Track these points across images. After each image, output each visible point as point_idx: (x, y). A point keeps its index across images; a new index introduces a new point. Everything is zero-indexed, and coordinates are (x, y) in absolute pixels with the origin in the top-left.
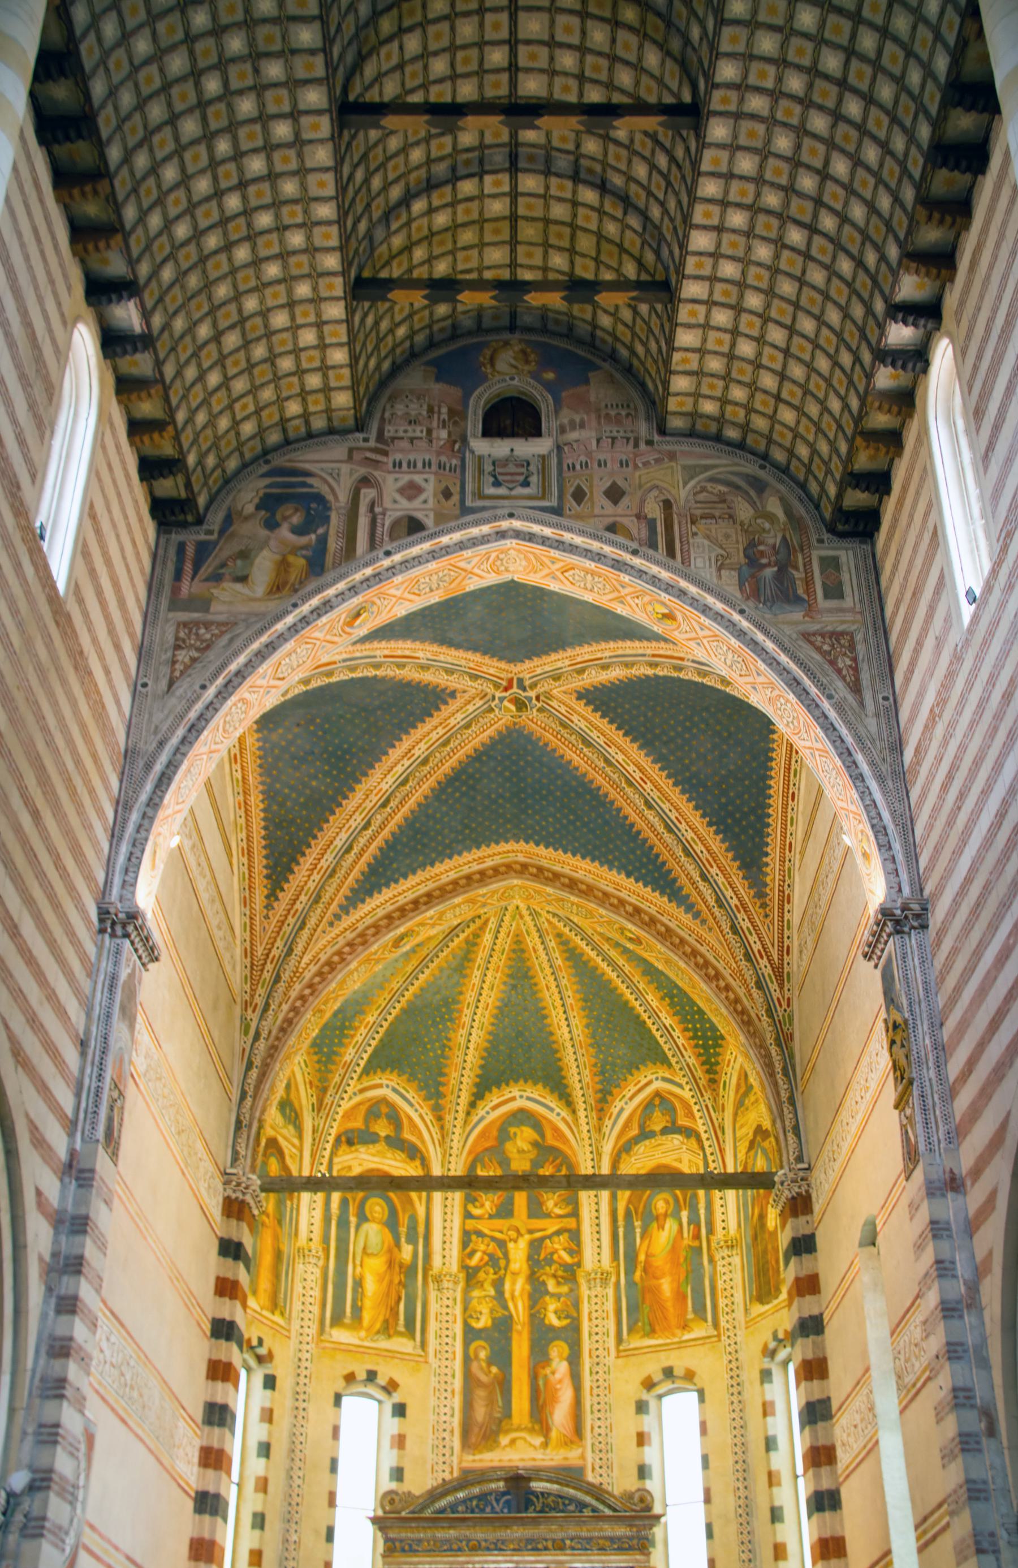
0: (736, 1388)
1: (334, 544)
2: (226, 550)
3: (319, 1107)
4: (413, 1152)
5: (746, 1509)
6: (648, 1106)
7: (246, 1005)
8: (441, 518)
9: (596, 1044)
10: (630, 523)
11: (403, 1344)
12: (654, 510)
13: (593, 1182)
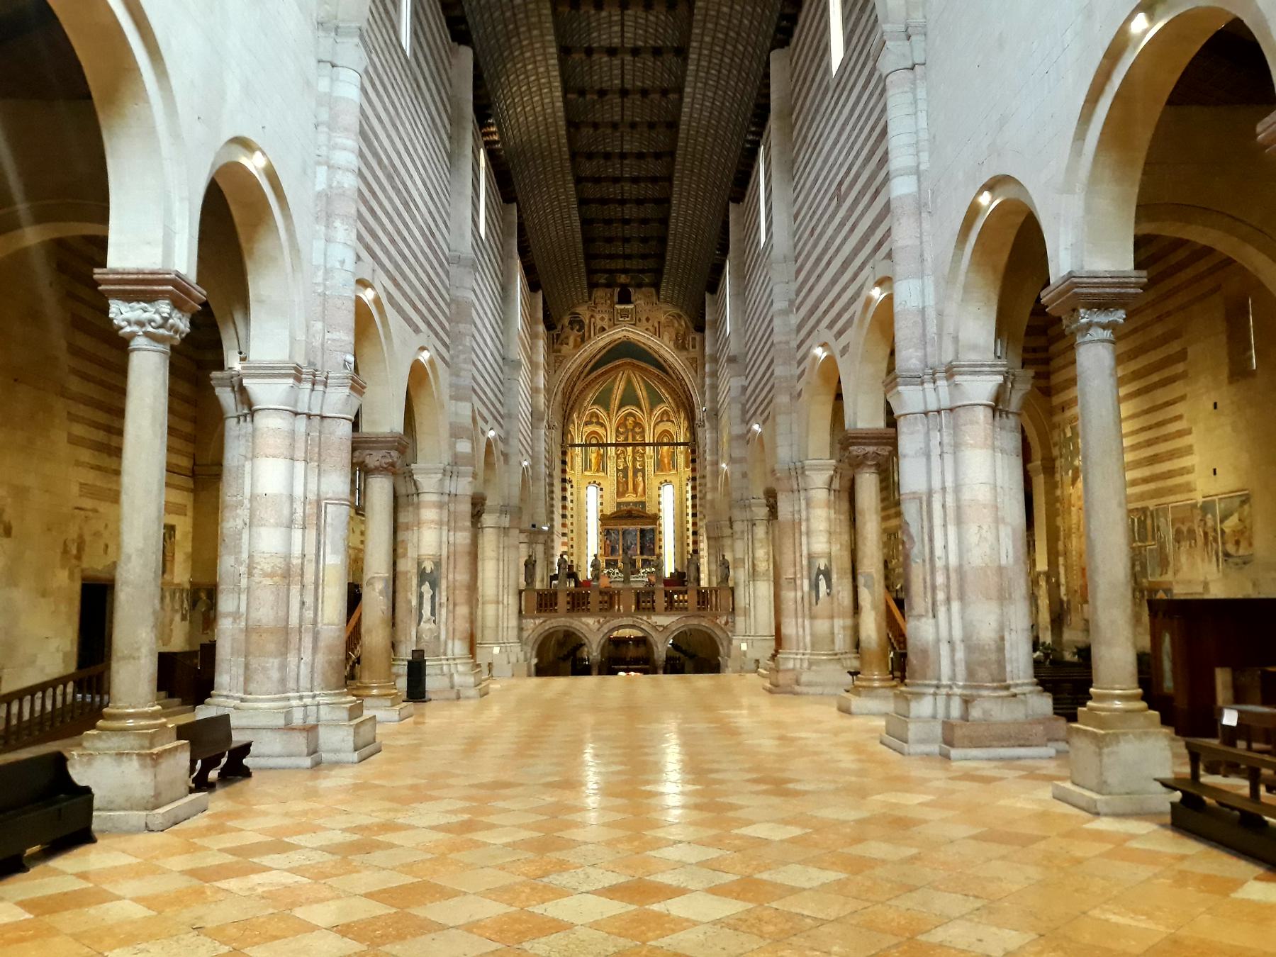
0: (681, 485)
1: (586, 335)
2: (563, 336)
3: (578, 417)
4: (602, 425)
5: (682, 512)
6: (663, 414)
7: (563, 403)
8: (609, 327)
9: (649, 398)
10: (651, 328)
11: (602, 474)
12: (656, 325)
13: (649, 444)
